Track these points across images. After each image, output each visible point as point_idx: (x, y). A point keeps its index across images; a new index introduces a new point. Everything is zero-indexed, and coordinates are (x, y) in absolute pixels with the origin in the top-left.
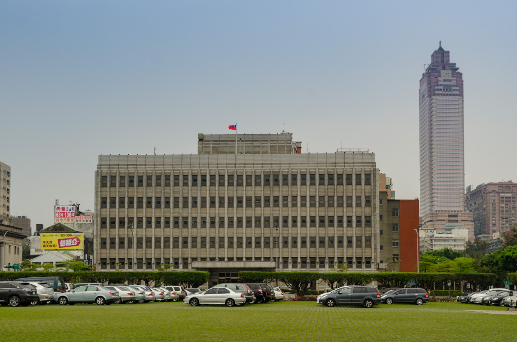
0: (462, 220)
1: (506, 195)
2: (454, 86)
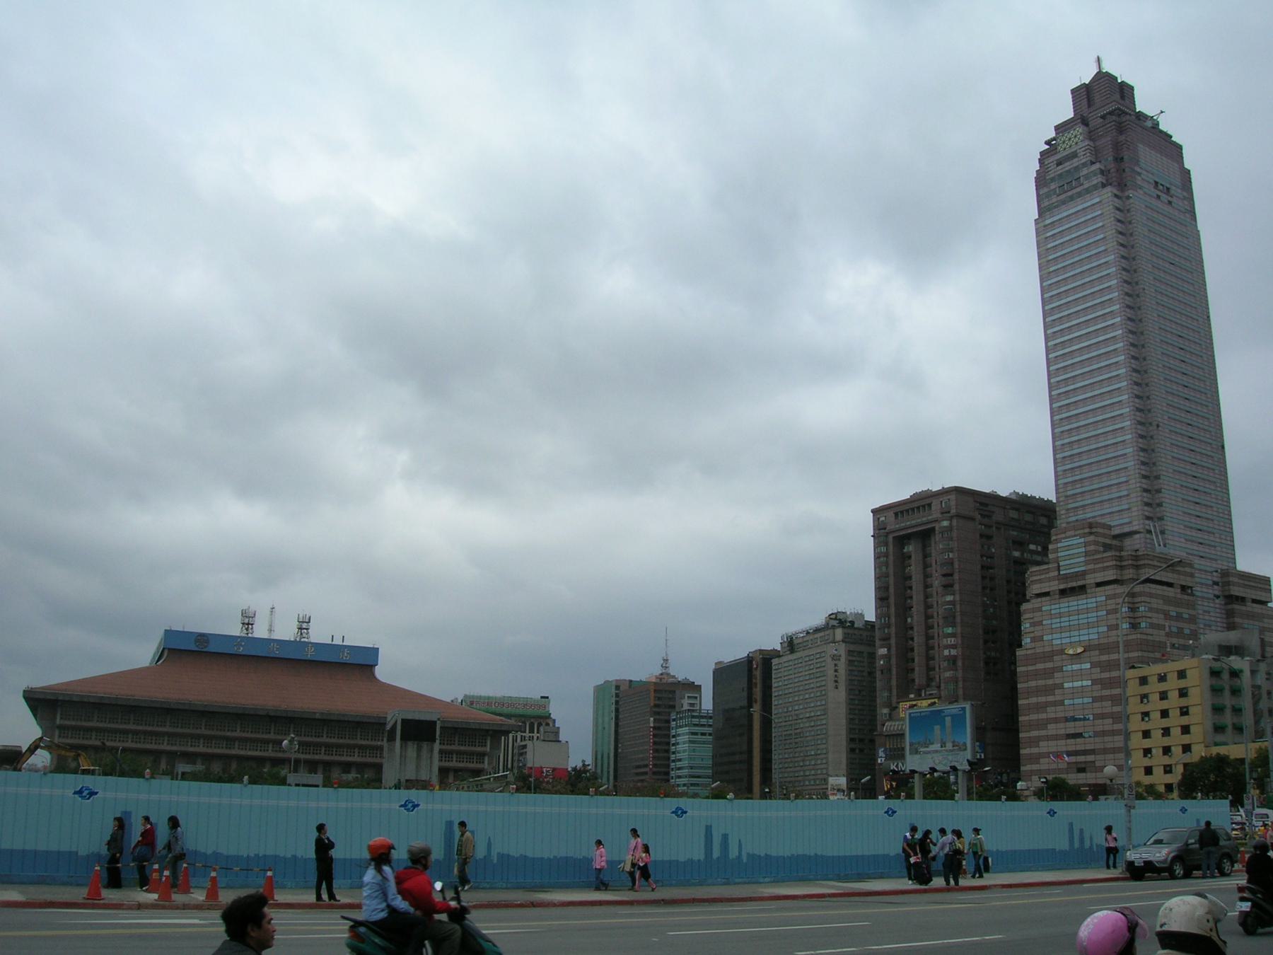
0: (1099, 585)
2: (1084, 165)
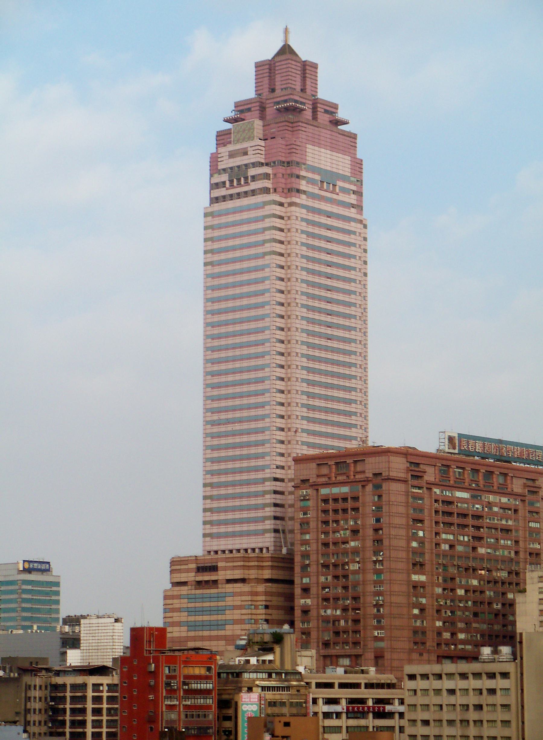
0: (229, 581)
1: (335, 490)
